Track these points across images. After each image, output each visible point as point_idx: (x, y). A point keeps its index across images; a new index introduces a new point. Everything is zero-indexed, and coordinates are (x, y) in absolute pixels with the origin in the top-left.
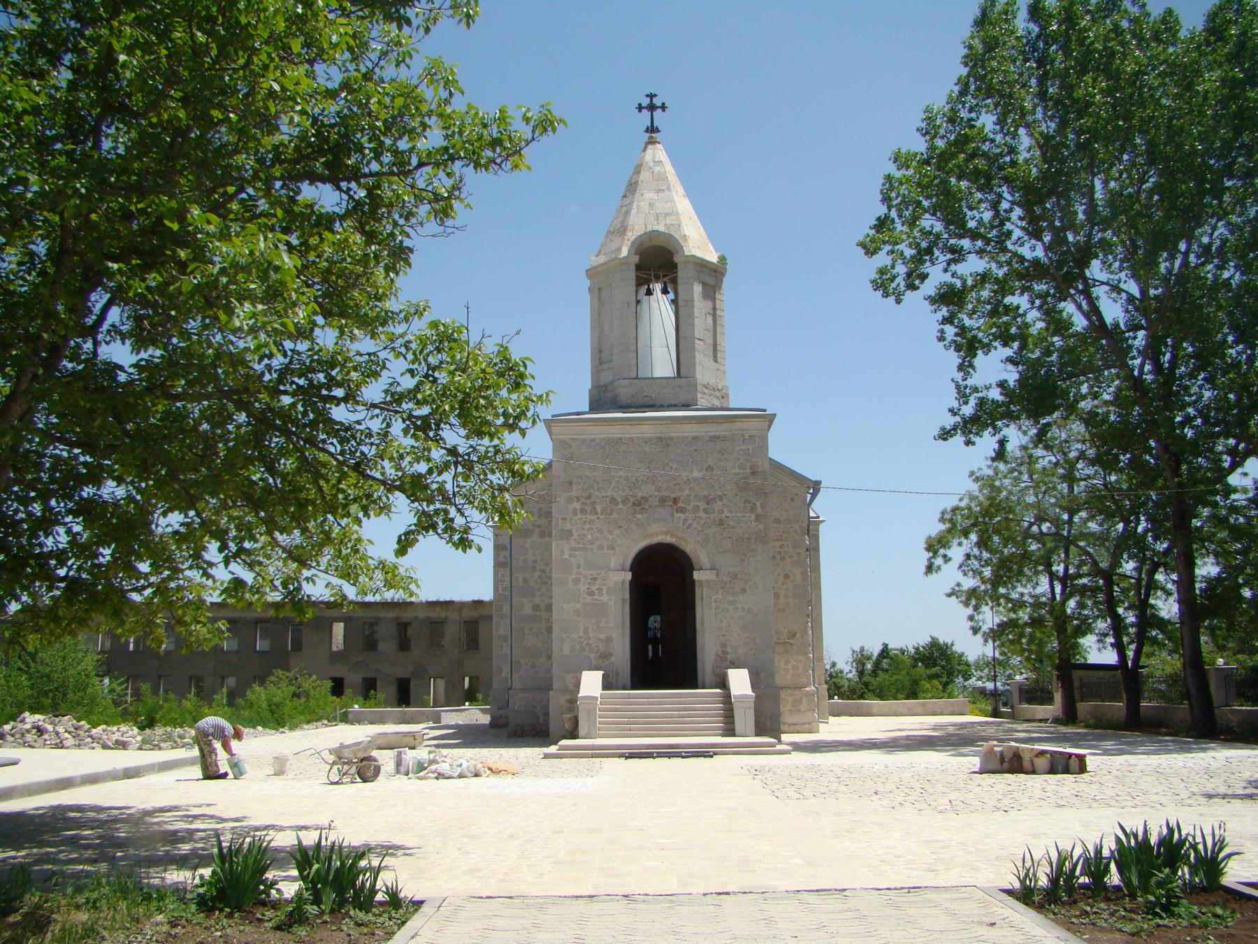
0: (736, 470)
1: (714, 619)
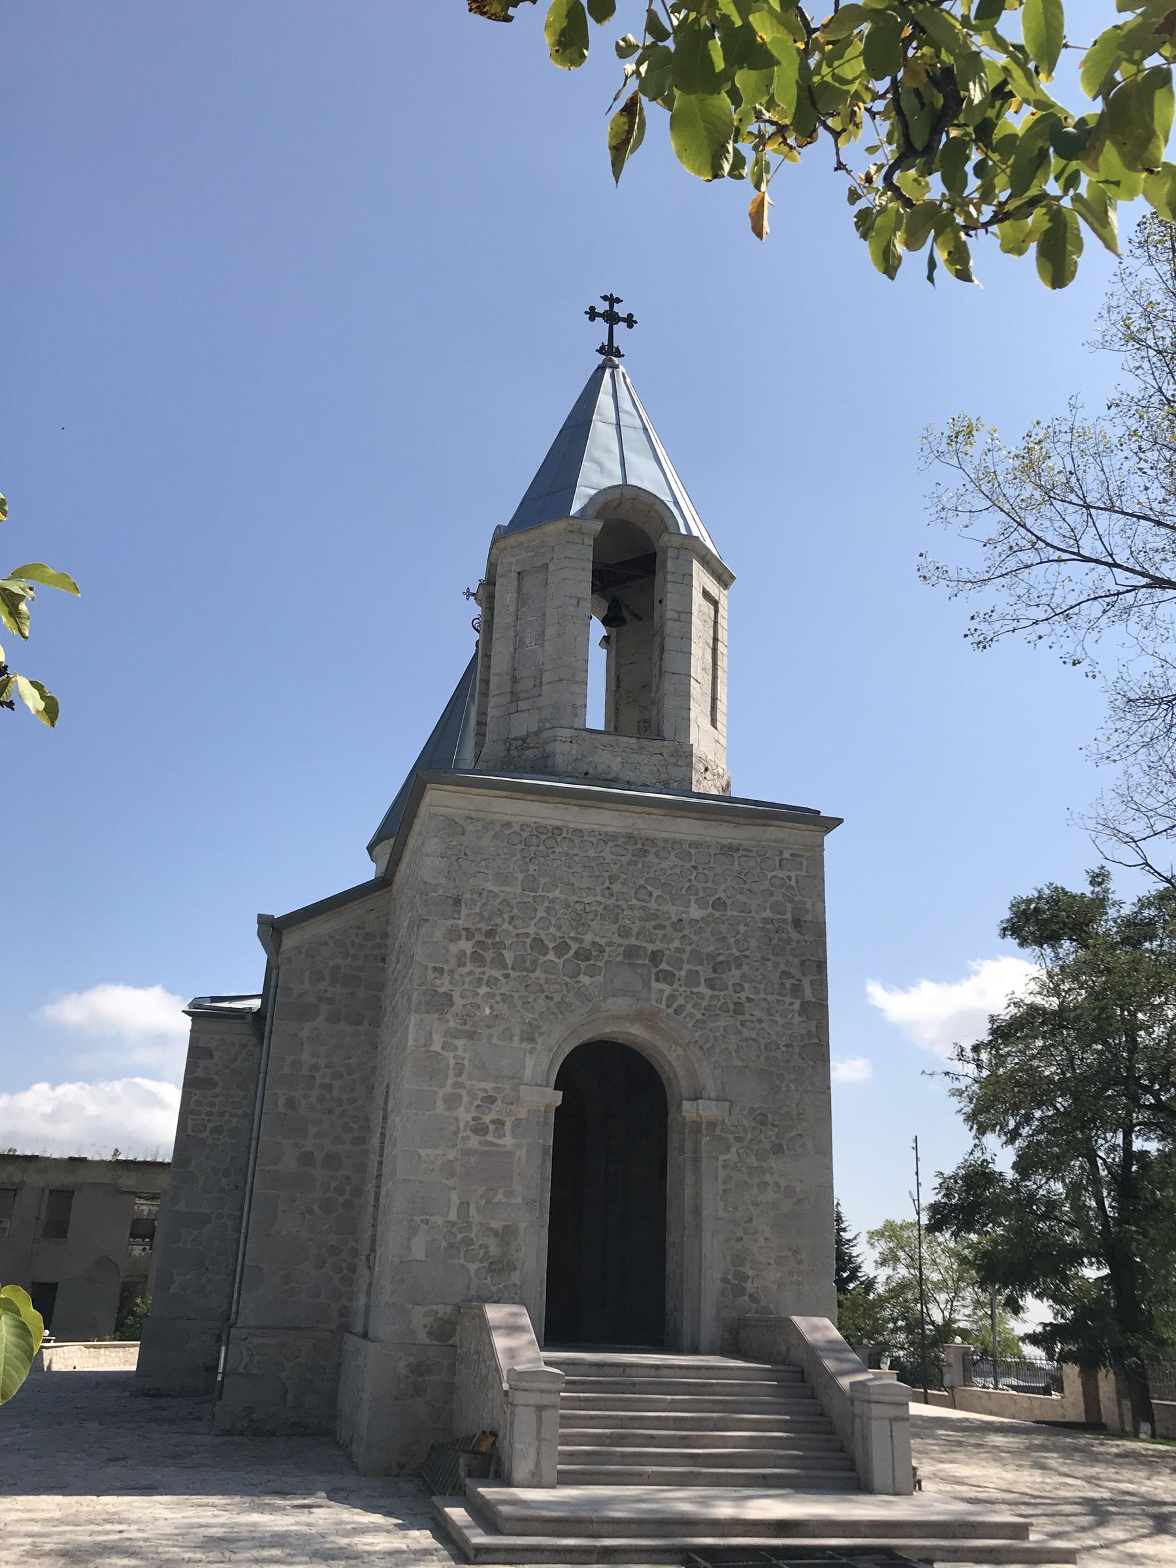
0: (768, 914)
1: (720, 1204)
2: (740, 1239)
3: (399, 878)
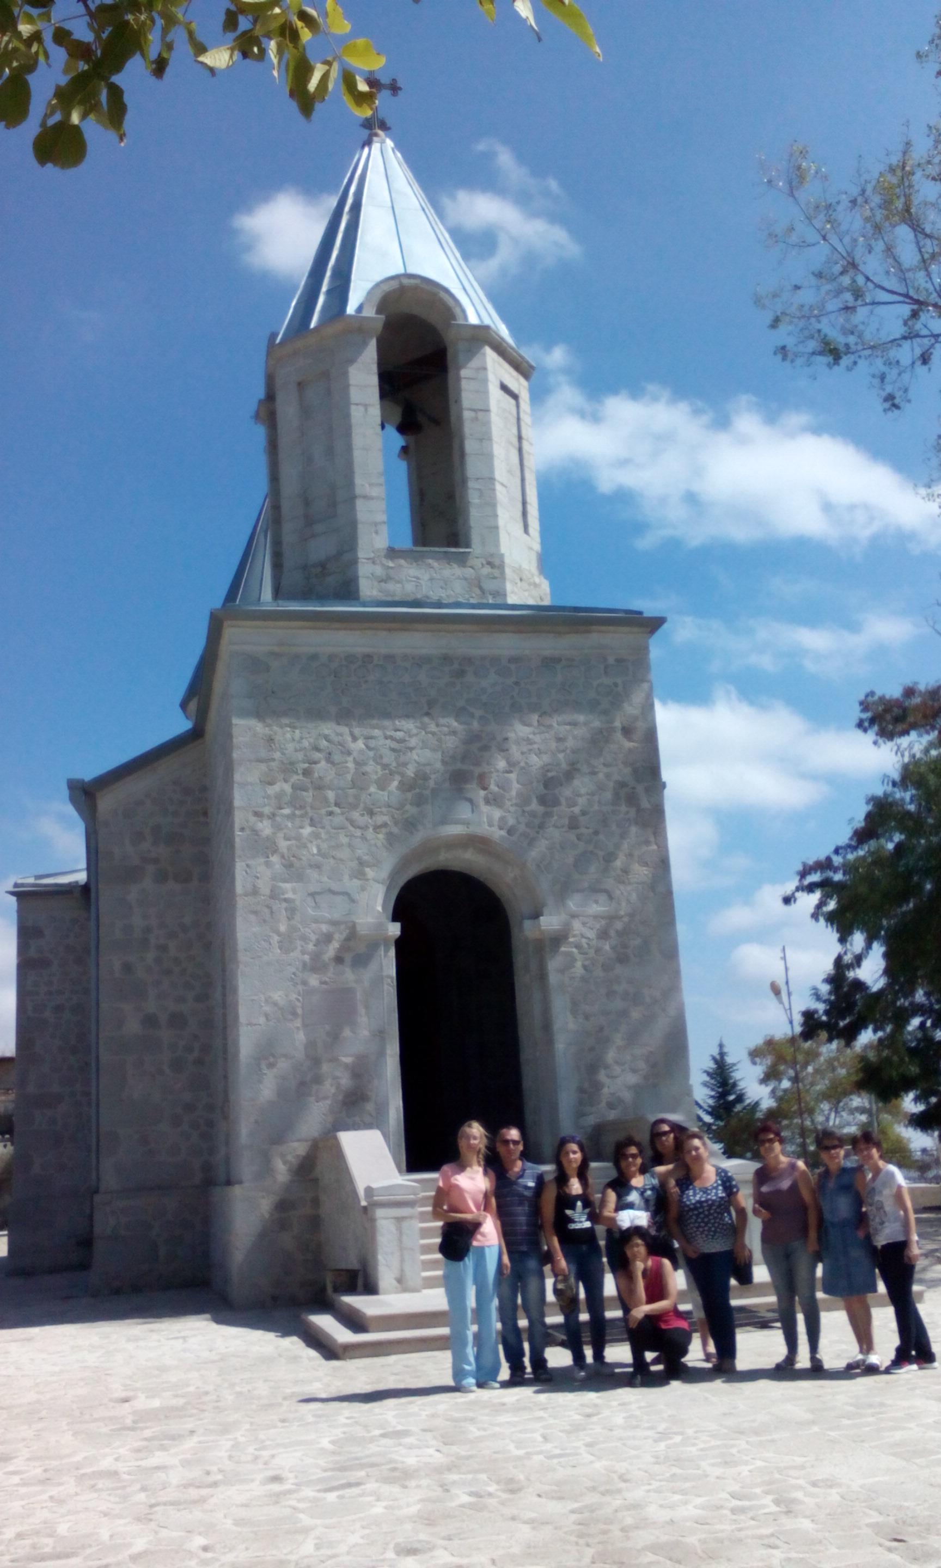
3: (210, 728)
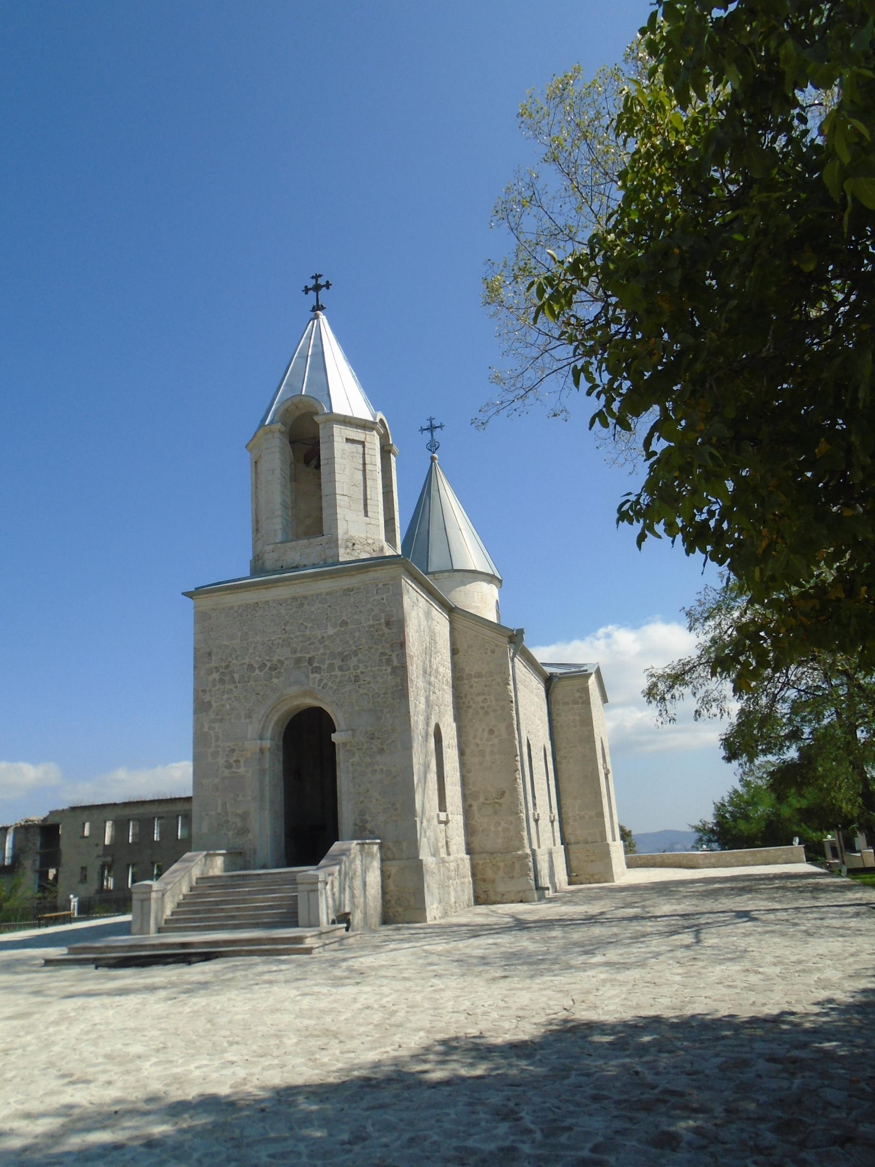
0: (371, 622)
2: (362, 802)
